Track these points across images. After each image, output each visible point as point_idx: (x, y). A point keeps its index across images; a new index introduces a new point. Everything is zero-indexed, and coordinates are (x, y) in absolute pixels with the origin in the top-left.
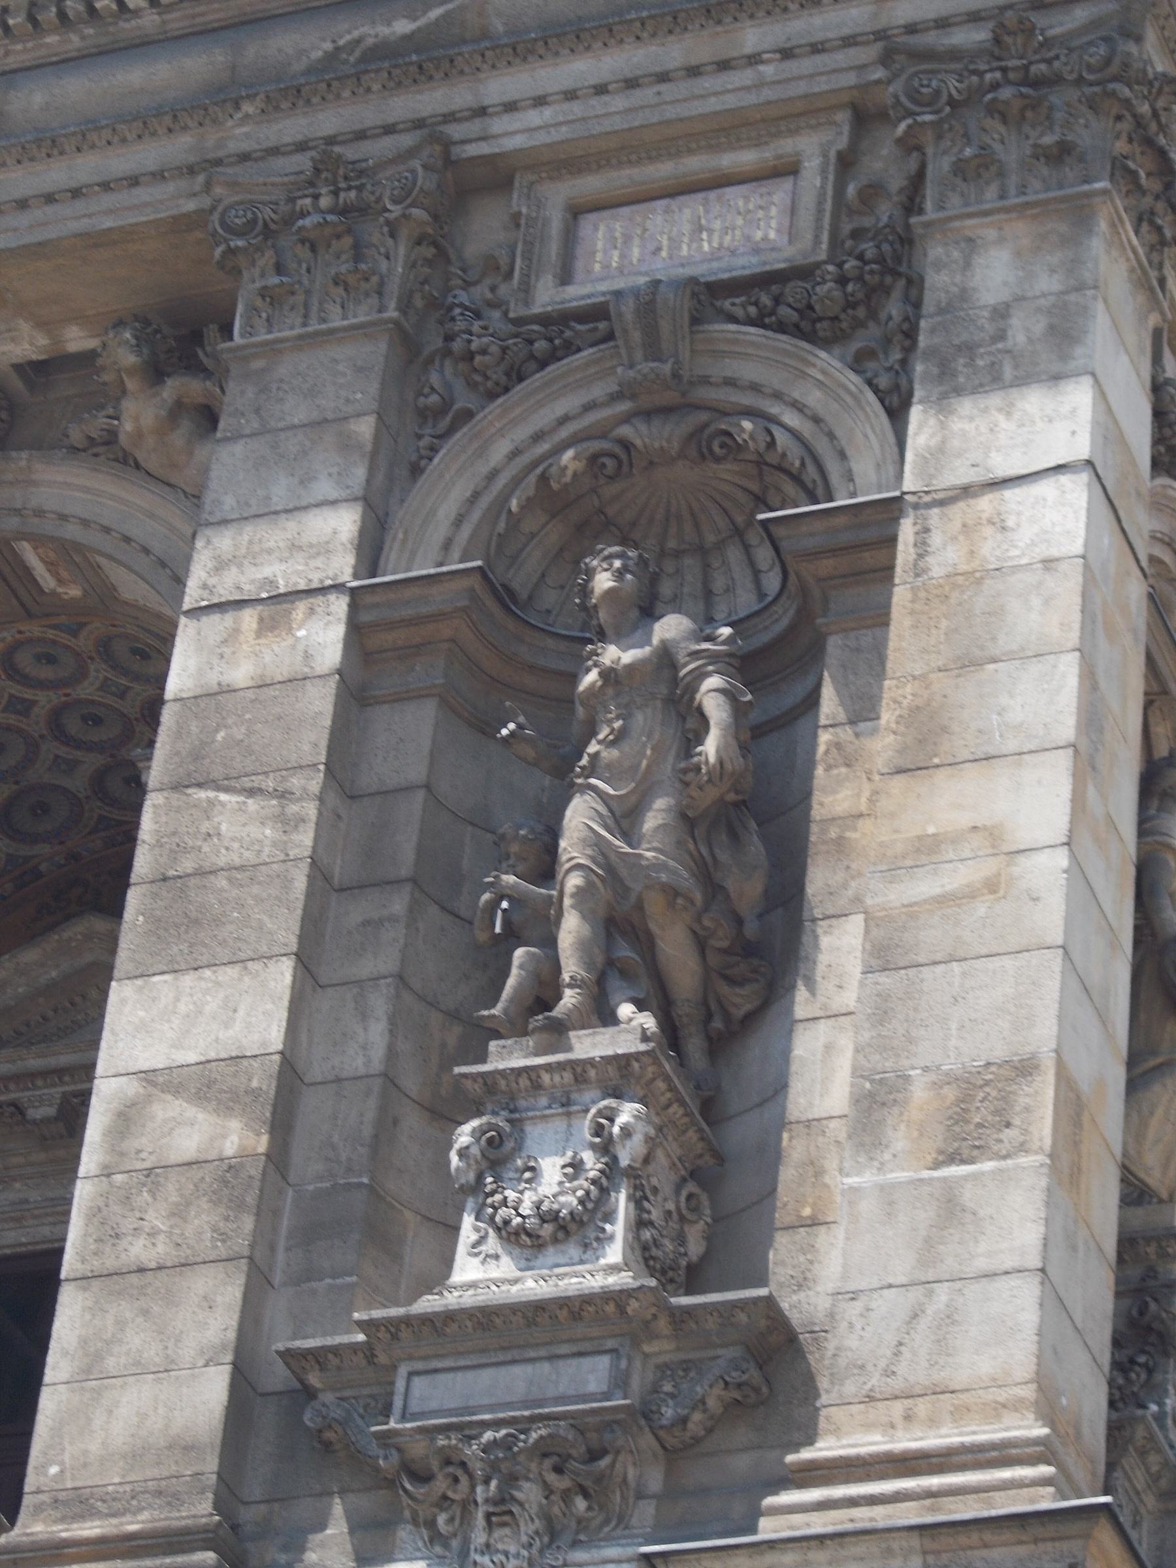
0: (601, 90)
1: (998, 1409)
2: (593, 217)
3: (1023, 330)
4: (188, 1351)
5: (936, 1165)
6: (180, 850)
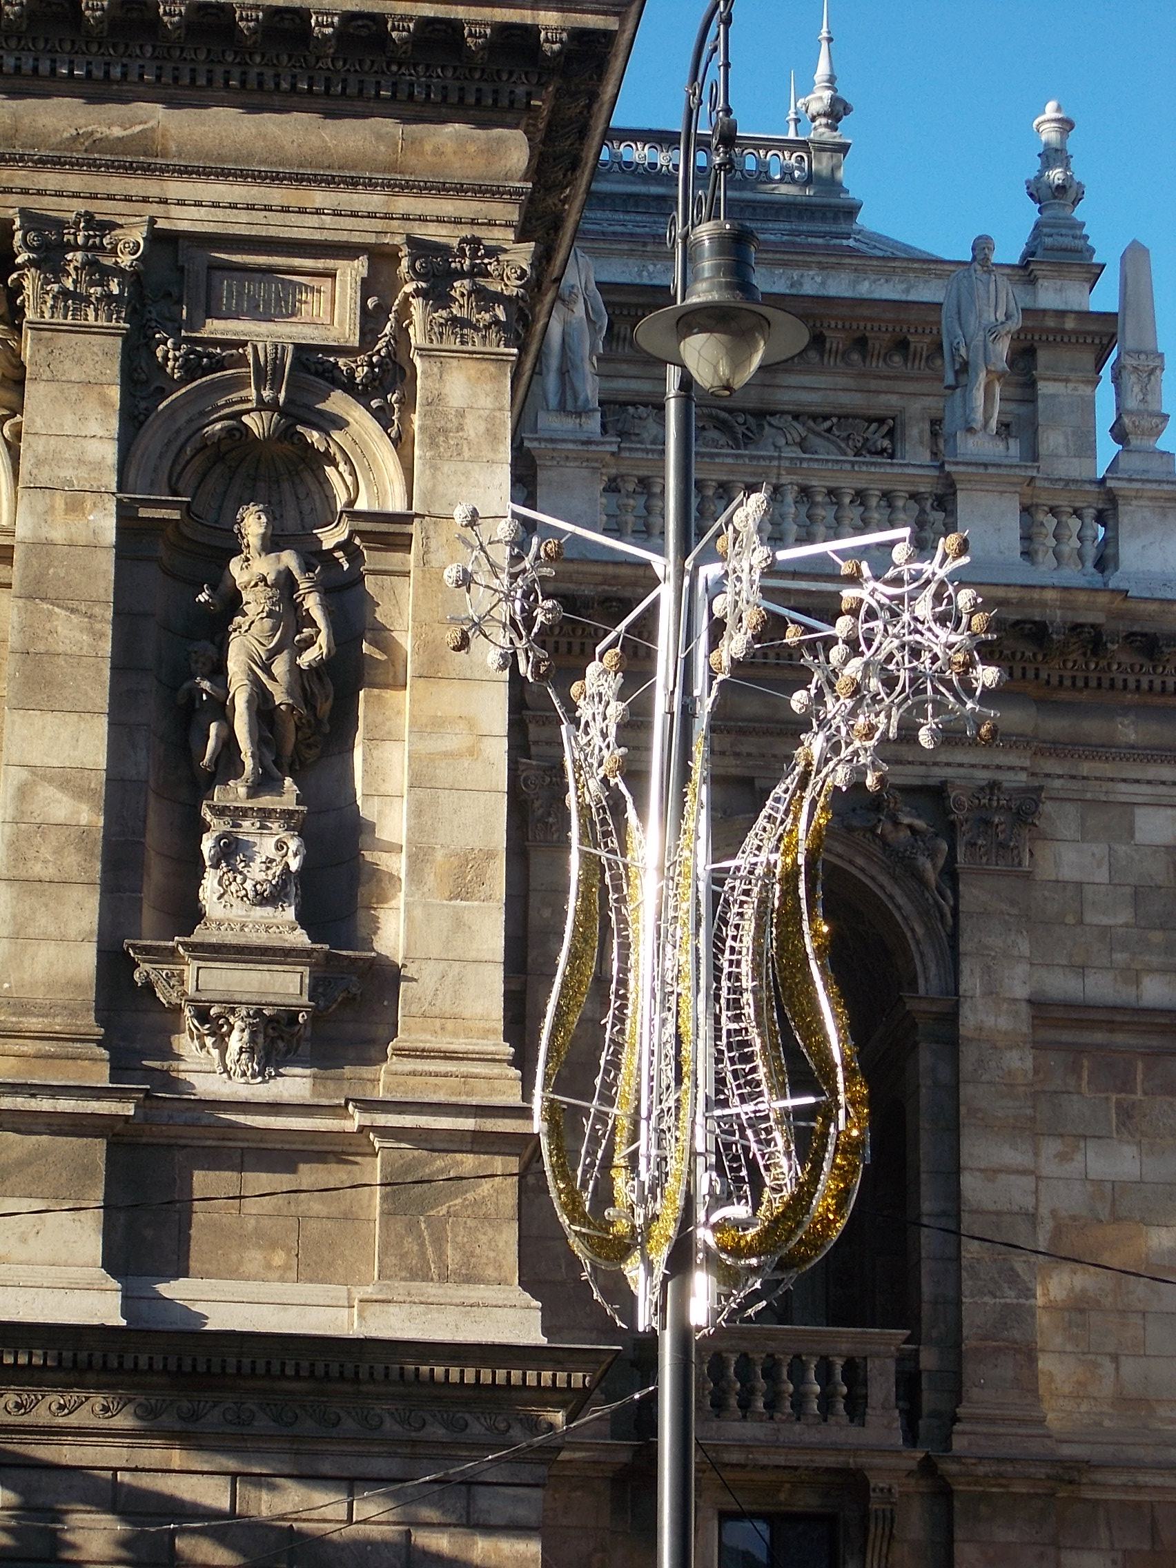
0: (233, 206)
1: (486, 1033)
2: (219, 273)
3: (474, 427)
4: (72, 932)
5: (451, 899)
6: (34, 637)
